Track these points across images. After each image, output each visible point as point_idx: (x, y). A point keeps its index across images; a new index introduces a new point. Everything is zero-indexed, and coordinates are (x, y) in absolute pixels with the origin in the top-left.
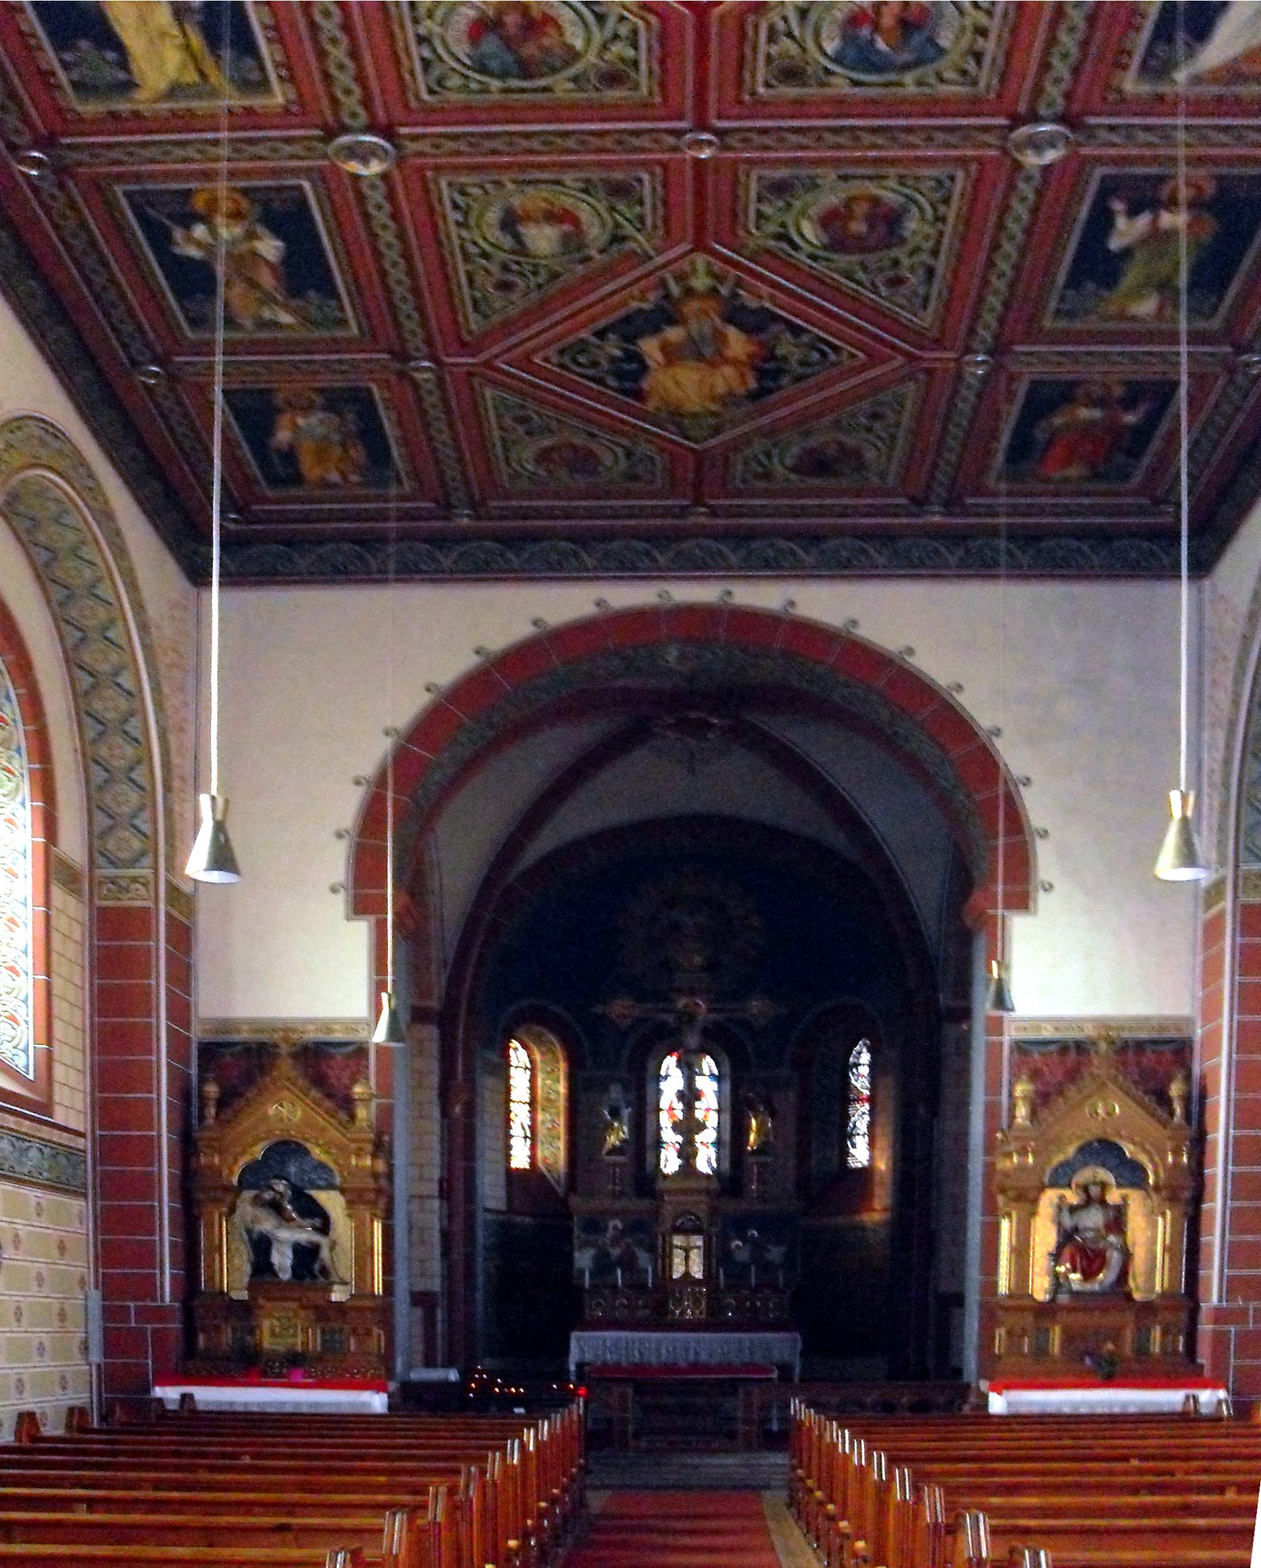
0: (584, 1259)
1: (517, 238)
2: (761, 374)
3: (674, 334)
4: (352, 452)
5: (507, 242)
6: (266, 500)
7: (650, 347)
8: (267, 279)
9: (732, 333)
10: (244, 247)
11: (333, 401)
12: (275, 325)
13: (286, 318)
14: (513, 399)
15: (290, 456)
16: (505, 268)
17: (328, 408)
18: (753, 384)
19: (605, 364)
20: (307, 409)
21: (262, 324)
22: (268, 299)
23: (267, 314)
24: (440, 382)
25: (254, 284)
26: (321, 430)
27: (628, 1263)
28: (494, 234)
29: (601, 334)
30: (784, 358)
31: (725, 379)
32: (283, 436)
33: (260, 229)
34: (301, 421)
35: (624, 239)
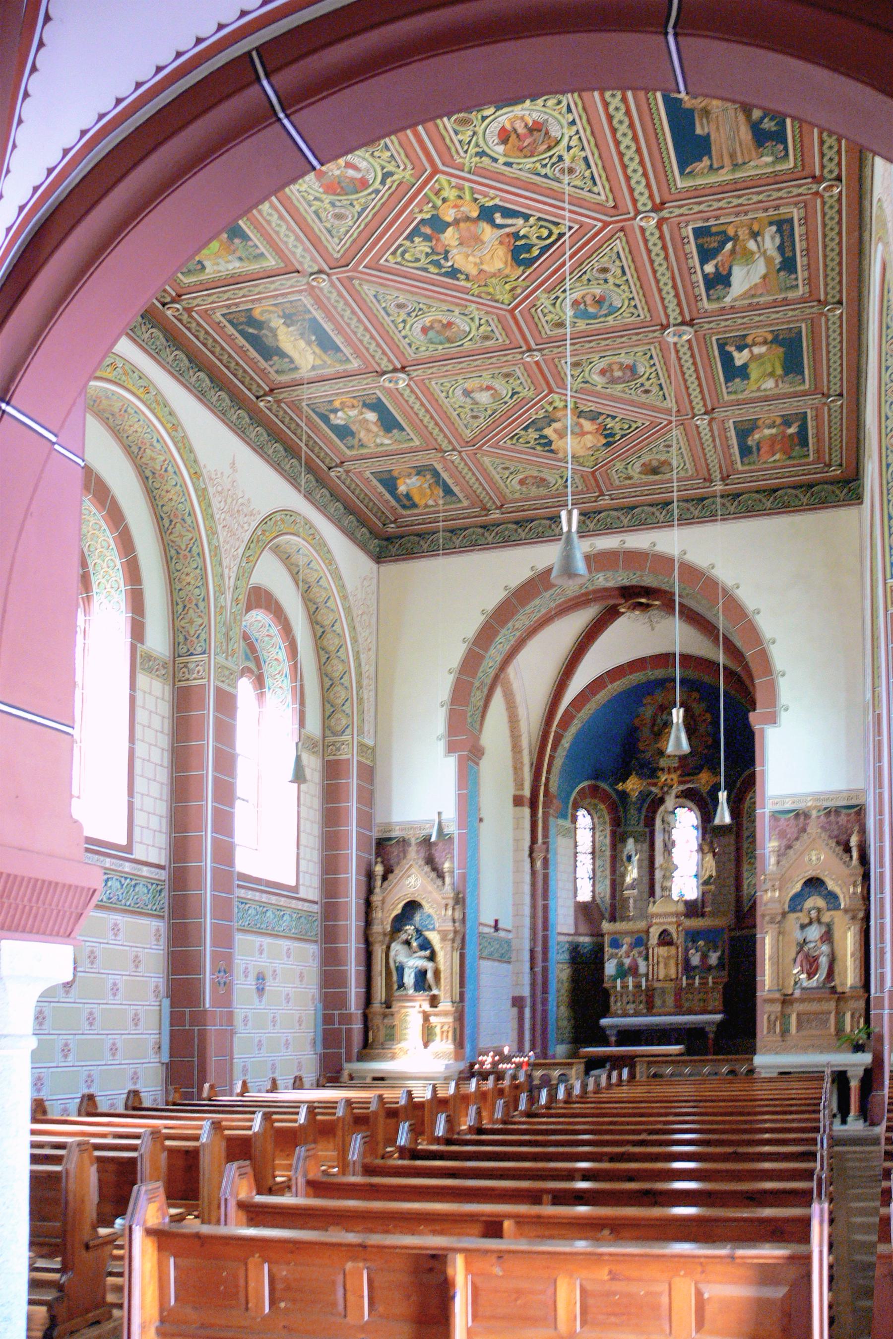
0: (610, 968)
1: (472, 398)
2: (606, 436)
3: (555, 425)
4: (436, 492)
5: (468, 400)
6: (403, 516)
7: (548, 432)
8: (375, 429)
9: (582, 421)
10: (361, 417)
11: (420, 471)
12: (382, 445)
13: (387, 442)
14: (497, 461)
15: (408, 496)
16: (472, 410)
17: (418, 474)
18: (604, 441)
19: (532, 442)
20: (409, 476)
21: (377, 446)
22: (377, 436)
23: (378, 441)
24: (462, 459)
25: (369, 431)
26: (418, 484)
27: (633, 970)
28: (462, 398)
29: (526, 429)
30: (611, 428)
31: (589, 440)
32: (402, 489)
33: (364, 410)
34: (408, 481)
35: (518, 393)
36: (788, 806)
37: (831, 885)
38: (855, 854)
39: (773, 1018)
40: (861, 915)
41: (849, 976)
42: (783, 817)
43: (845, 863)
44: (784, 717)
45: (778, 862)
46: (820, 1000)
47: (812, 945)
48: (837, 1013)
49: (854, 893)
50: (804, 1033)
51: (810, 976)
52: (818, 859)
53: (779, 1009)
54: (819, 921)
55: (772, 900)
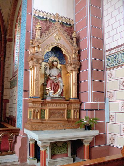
36: (42, 15)
37: (64, 52)
38: (75, 41)
39: (36, 111)
40: (78, 67)
41: (73, 94)
42: (40, 19)
43: (71, 43)
46: (60, 103)
47: (54, 78)
48: (68, 110)
50: (52, 119)
51: (55, 91)
53: (40, 107)
54: (57, 68)
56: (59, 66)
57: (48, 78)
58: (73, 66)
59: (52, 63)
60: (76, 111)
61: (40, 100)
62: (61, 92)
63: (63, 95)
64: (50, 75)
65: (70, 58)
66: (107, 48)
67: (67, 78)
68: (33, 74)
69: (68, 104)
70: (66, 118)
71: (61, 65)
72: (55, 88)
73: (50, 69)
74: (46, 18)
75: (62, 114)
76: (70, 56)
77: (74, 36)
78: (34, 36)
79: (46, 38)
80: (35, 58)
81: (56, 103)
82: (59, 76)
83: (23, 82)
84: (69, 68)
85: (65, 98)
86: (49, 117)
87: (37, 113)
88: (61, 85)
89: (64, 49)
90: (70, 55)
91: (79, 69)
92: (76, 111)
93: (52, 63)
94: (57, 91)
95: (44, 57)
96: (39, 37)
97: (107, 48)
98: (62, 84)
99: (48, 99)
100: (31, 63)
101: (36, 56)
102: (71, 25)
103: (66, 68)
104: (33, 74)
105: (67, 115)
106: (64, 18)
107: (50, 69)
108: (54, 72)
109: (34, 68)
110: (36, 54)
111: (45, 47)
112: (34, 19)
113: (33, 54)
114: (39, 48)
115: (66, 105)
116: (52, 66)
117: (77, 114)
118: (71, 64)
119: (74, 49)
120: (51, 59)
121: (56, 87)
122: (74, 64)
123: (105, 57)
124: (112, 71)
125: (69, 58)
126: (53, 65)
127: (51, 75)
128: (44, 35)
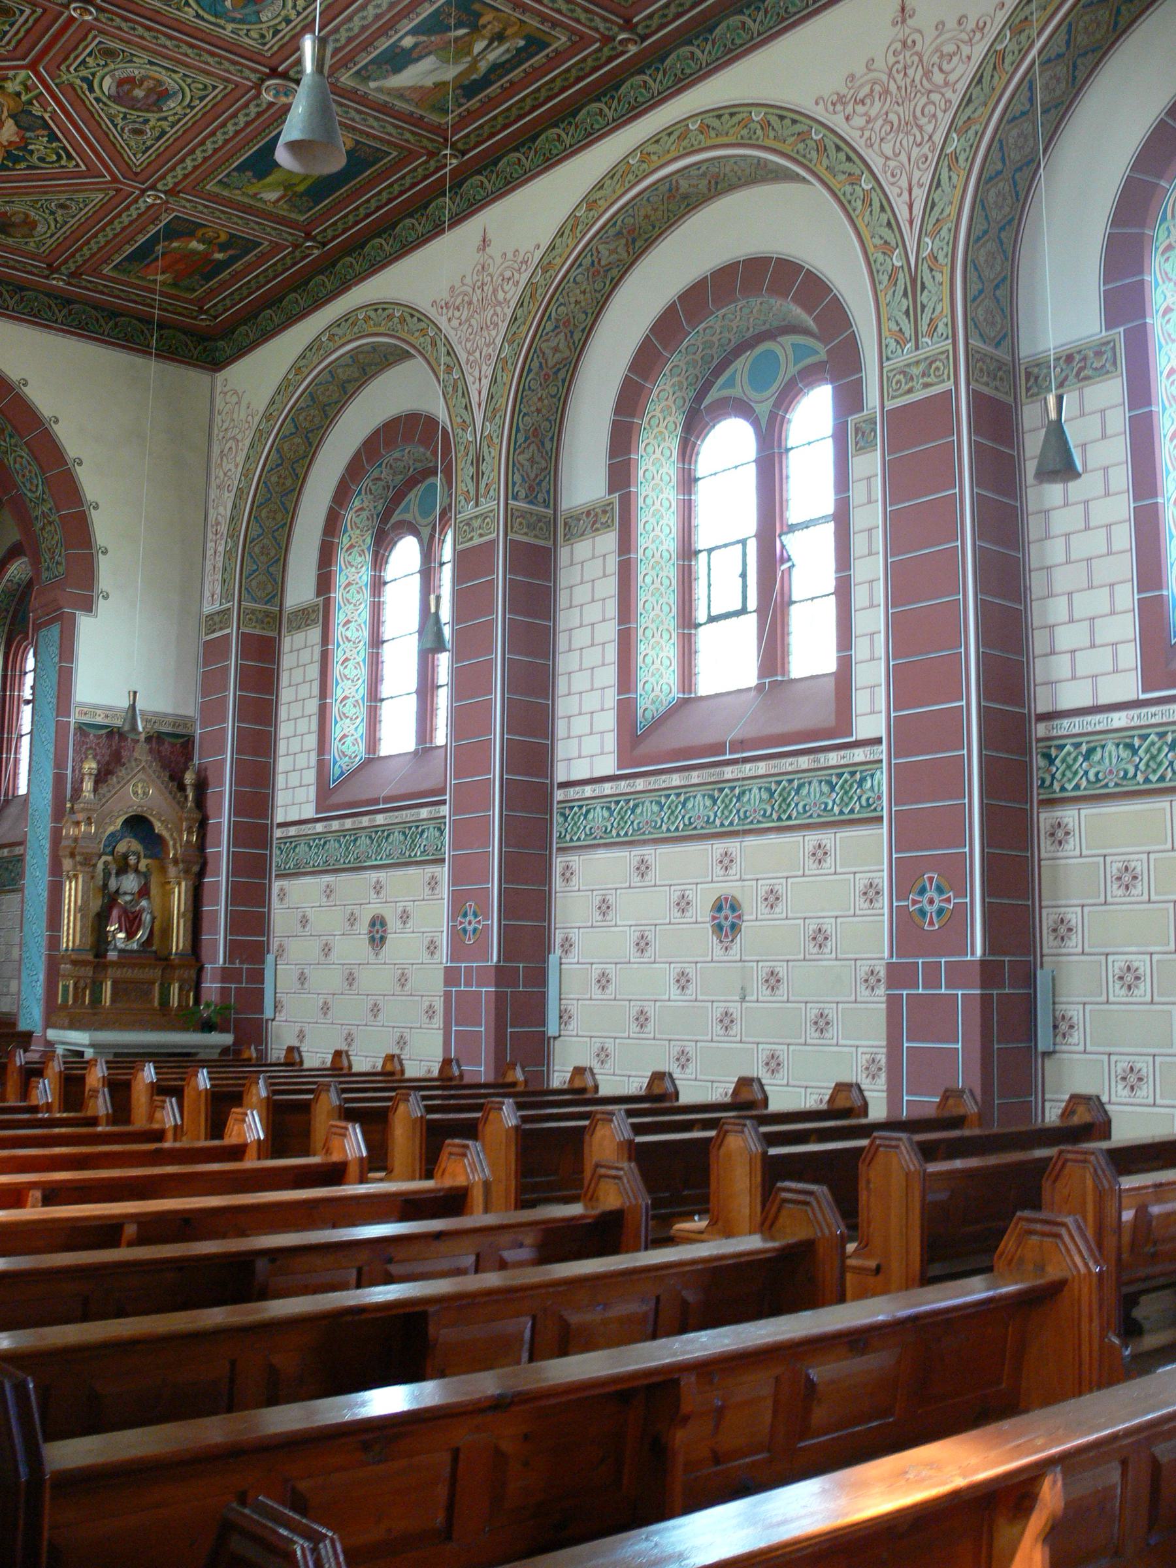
36: (99, 720)
37: (158, 827)
39: (82, 984)
40: (196, 869)
41: (178, 941)
42: (93, 731)
43: (179, 803)
44: (102, 605)
45: (95, 790)
46: (142, 966)
47: (128, 898)
48: (162, 985)
49: (188, 841)
50: (119, 1005)
51: (130, 935)
52: (145, 794)
53: (91, 974)
55: (87, 836)
56: (142, 866)
57: (111, 900)
58: (181, 866)
59: (125, 857)
60: (187, 987)
61: (90, 957)
62: (145, 938)
63: (152, 945)
64: (117, 891)
65: (175, 845)
66: (280, 818)
67: (167, 895)
68: (72, 892)
69: (164, 970)
70: (156, 1004)
71: (149, 861)
72: (131, 927)
73: (118, 874)
74: (107, 727)
75: (148, 994)
76: (174, 839)
77: (189, 778)
78: (77, 791)
79: (109, 795)
80: (80, 854)
81: (133, 966)
82: (144, 892)
83: (45, 910)
84: (172, 871)
85: (155, 952)
86: (113, 1001)
87: (84, 989)
88: (146, 917)
89: (159, 820)
90: (177, 841)
91: (201, 874)
92: (187, 987)
93: (125, 857)
94: (136, 934)
95: (102, 846)
96: (92, 796)
97: (280, 818)
98: (148, 917)
99: (112, 955)
100: (67, 864)
101: (82, 847)
102: (183, 736)
103: (163, 870)
104: (72, 892)
105: (161, 998)
106: (165, 715)
107: (118, 874)
108: (130, 883)
109: (76, 876)
110: (81, 843)
111: (107, 820)
112: (75, 735)
113: (76, 840)
114: (90, 824)
115: (158, 972)
116: (123, 868)
117: (188, 997)
118: (175, 861)
119: (187, 819)
120: (122, 847)
121: (131, 923)
122: (183, 861)
123: (275, 842)
124: (284, 883)
125: (171, 843)
126: (127, 864)
127: (121, 891)
128: (103, 789)
